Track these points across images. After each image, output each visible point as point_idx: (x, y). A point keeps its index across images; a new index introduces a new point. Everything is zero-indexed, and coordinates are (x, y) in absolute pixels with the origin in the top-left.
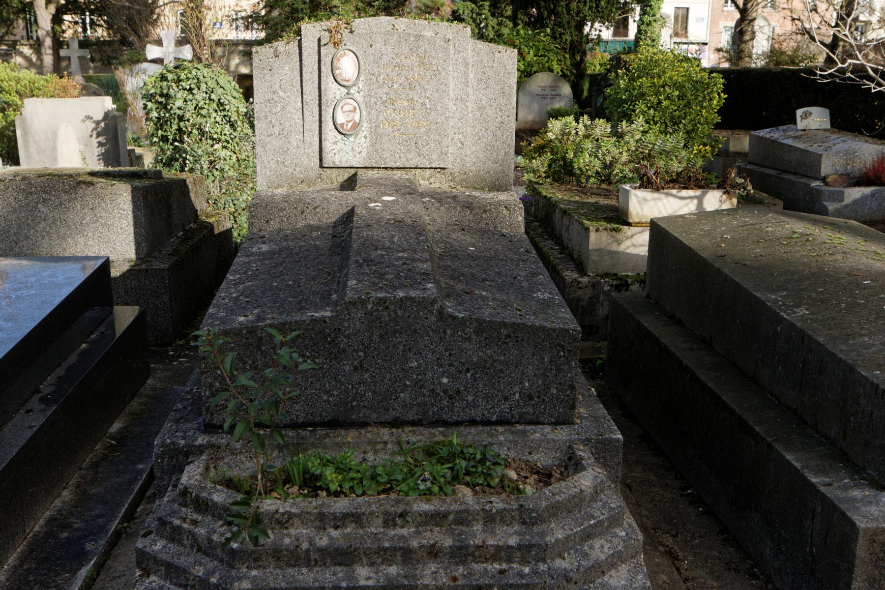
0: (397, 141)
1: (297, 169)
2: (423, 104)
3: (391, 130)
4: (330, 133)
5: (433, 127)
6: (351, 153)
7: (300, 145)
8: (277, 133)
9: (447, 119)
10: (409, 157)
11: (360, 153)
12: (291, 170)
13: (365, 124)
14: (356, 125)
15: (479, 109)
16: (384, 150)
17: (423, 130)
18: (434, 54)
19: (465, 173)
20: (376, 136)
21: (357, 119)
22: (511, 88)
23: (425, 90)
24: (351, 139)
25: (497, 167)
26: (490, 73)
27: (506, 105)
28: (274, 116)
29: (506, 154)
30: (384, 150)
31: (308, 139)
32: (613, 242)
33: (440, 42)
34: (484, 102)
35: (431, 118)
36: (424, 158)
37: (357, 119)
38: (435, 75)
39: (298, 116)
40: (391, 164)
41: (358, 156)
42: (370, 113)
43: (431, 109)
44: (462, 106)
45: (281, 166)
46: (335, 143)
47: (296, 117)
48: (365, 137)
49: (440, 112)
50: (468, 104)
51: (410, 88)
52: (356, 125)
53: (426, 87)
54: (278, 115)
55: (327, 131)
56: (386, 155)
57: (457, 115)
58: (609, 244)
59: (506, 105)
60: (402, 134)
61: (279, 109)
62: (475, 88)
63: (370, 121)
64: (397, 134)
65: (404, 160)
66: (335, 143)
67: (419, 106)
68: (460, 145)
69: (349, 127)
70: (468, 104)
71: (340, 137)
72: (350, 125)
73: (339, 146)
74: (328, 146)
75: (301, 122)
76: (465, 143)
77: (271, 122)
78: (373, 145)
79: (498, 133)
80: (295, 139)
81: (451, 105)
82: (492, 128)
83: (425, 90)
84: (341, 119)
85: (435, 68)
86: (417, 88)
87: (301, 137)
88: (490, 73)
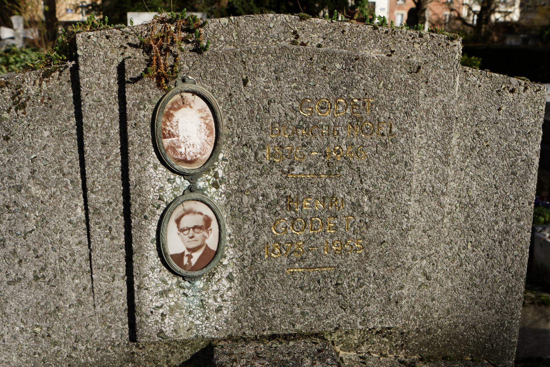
0: (298, 282)
1: (81, 347)
2: (356, 206)
3: (285, 261)
4: (153, 275)
5: (375, 250)
6: (198, 313)
7: (84, 296)
8: (30, 275)
9: (404, 233)
10: (322, 312)
11: (219, 310)
12: (65, 351)
13: (230, 252)
14: (210, 258)
15: (463, 207)
16: (269, 302)
17: (353, 257)
18: (384, 97)
19: (429, 332)
20: (252, 274)
21: (212, 242)
22: (528, 162)
23: (362, 176)
24: (199, 284)
25: (491, 316)
26: (491, 134)
27: (517, 198)
28: (21, 240)
29: (509, 291)
30: (269, 302)
31: (102, 285)
32: (541, 318)
33: (400, 74)
34: (473, 193)
35: (371, 232)
36: (353, 312)
37: (212, 242)
38: (385, 145)
39: (75, 239)
40: (284, 328)
41: (214, 316)
42: (240, 228)
43: (371, 215)
44: (433, 204)
45: (44, 343)
46: (164, 293)
47: (73, 240)
48: (230, 278)
49: (391, 219)
50: (446, 200)
51: (329, 173)
52: (210, 258)
53: (364, 169)
54: (31, 238)
55: (146, 269)
56: (273, 310)
57: (422, 223)
58: (536, 321)
59: (517, 198)
60: (309, 267)
61: (31, 225)
62: (459, 165)
63: (240, 245)
64: (298, 269)
65: (312, 319)
66: (164, 293)
67: (346, 210)
68: (422, 279)
69: (194, 261)
70: (446, 200)
71: (173, 281)
72: (196, 256)
73: (171, 300)
74: (148, 300)
75: (85, 250)
76: (434, 276)
77: (14, 252)
78: (246, 293)
79: (498, 252)
80: (71, 287)
81: (414, 208)
82: (487, 243)
83: (362, 176)
84: (175, 244)
85: (385, 129)
86: (344, 171)
87: (85, 281)
88: (491, 134)
